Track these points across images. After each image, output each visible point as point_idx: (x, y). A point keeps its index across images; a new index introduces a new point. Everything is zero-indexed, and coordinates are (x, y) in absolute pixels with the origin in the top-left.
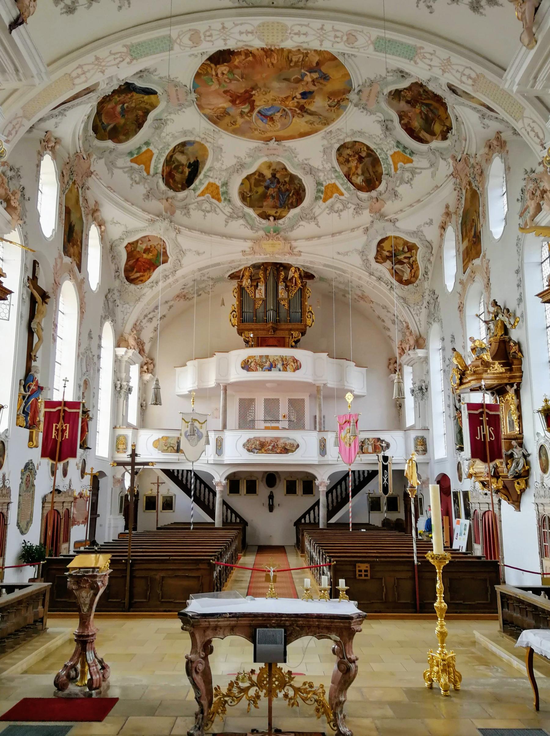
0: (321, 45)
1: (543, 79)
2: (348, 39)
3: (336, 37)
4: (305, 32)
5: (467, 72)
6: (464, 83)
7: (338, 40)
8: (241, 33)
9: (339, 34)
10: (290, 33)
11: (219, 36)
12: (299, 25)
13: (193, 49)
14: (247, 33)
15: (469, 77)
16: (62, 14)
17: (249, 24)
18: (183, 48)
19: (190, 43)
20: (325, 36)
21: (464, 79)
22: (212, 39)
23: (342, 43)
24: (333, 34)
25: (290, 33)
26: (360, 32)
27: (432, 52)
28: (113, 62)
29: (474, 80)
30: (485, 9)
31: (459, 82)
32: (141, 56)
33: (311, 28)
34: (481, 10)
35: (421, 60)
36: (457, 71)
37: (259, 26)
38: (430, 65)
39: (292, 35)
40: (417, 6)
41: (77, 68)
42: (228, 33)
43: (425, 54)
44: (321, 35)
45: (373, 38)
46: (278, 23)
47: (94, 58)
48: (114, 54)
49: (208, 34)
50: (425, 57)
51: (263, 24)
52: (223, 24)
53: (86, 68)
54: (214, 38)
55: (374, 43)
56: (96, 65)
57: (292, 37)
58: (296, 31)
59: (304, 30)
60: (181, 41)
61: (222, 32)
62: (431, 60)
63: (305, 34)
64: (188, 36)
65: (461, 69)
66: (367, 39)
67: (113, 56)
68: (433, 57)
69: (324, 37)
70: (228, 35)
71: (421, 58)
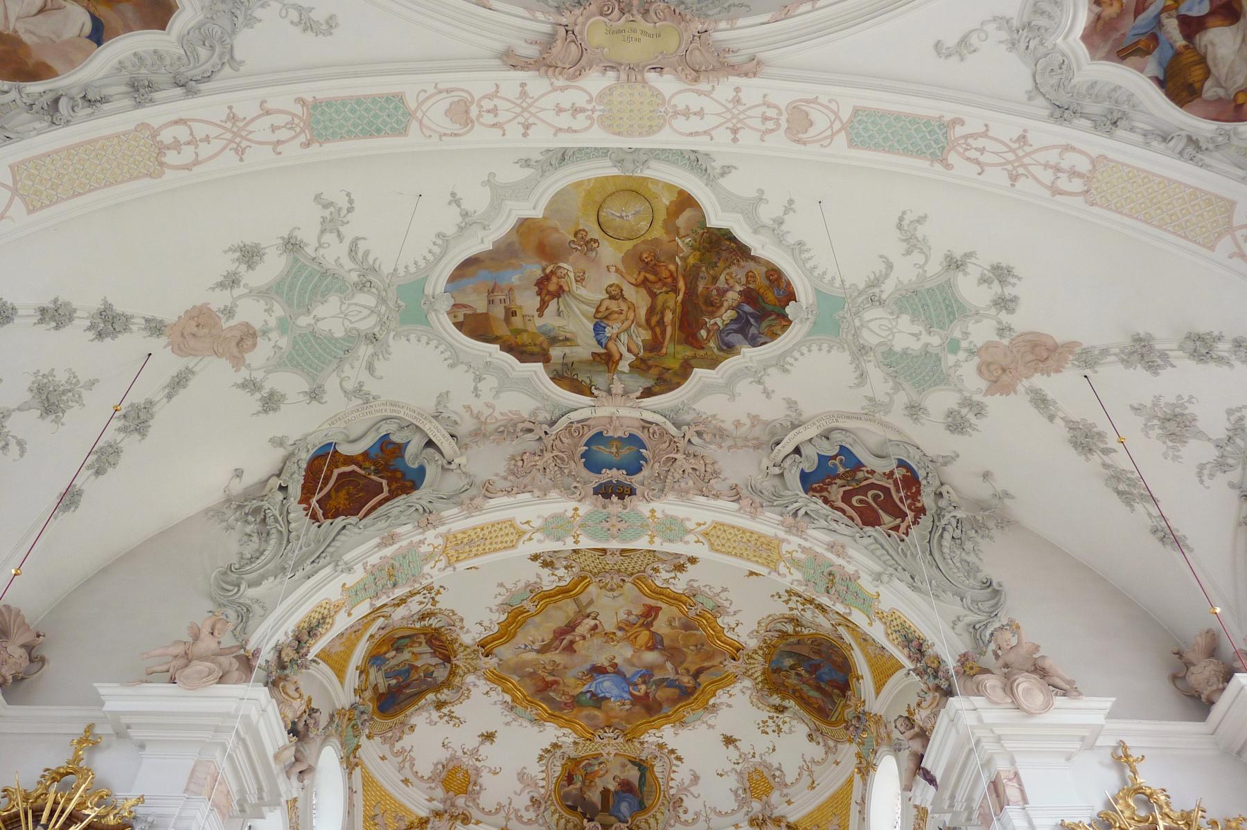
0: (523, 85)
1: (235, 752)
2: (467, 112)
3: (494, 111)
4: (563, 114)
5: (188, 154)
6: (176, 122)
7: (487, 104)
8: (700, 114)
9: (488, 119)
10: (593, 111)
11: (749, 113)
12: (575, 131)
13: (812, 97)
14: (687, 113)
15: (177, 145)
16: (1020, 279)
17: (681, 133)
18: (834, 106)
19: (814, 115)
20: (518, 110)
21: (182, 133)
22: (764, 108)
23: (476, 98)
24: (502, 117)
25: (593, 111)
26: (445, 134)
27: (280, 148)
28: (990, 145)
29: (162, 149)
30: (233, 261)
31: (184, 116)
32: (928, 123)
33: (549, 124)
34: (238, 254)
35: (294, 115)
36: (207, 139)
37: (661, 127)
38: (268, 113)
39: (589, 107)
40: (348, 195)
41: (1062, 193)
42: (729, 116)
43: (292, 133)
44: (524, 110)
45: (414, 125)
46: (619, 134)
47: (1018, 185)
48: (977, 162)
49: (770, 125)
50: (290, 126)
51: (651, 131)
52: (735, 140)
53: (1047, 176)
54: (758, 112)
55: (410, 115)
56: (1024, 166)
57: (590, 102)
58: (581, 116)
59: (564, 120)
60: (832, 123)
61: (740, 121)
62: (274, 128)
63: (559, 110)
64: (812, 132)
65: (205, 150)
66: (425, 121)
67: (982, 159)
68: (274, 138)
69: (519, 105)
70: (728, 110)
71: (297, 121)
